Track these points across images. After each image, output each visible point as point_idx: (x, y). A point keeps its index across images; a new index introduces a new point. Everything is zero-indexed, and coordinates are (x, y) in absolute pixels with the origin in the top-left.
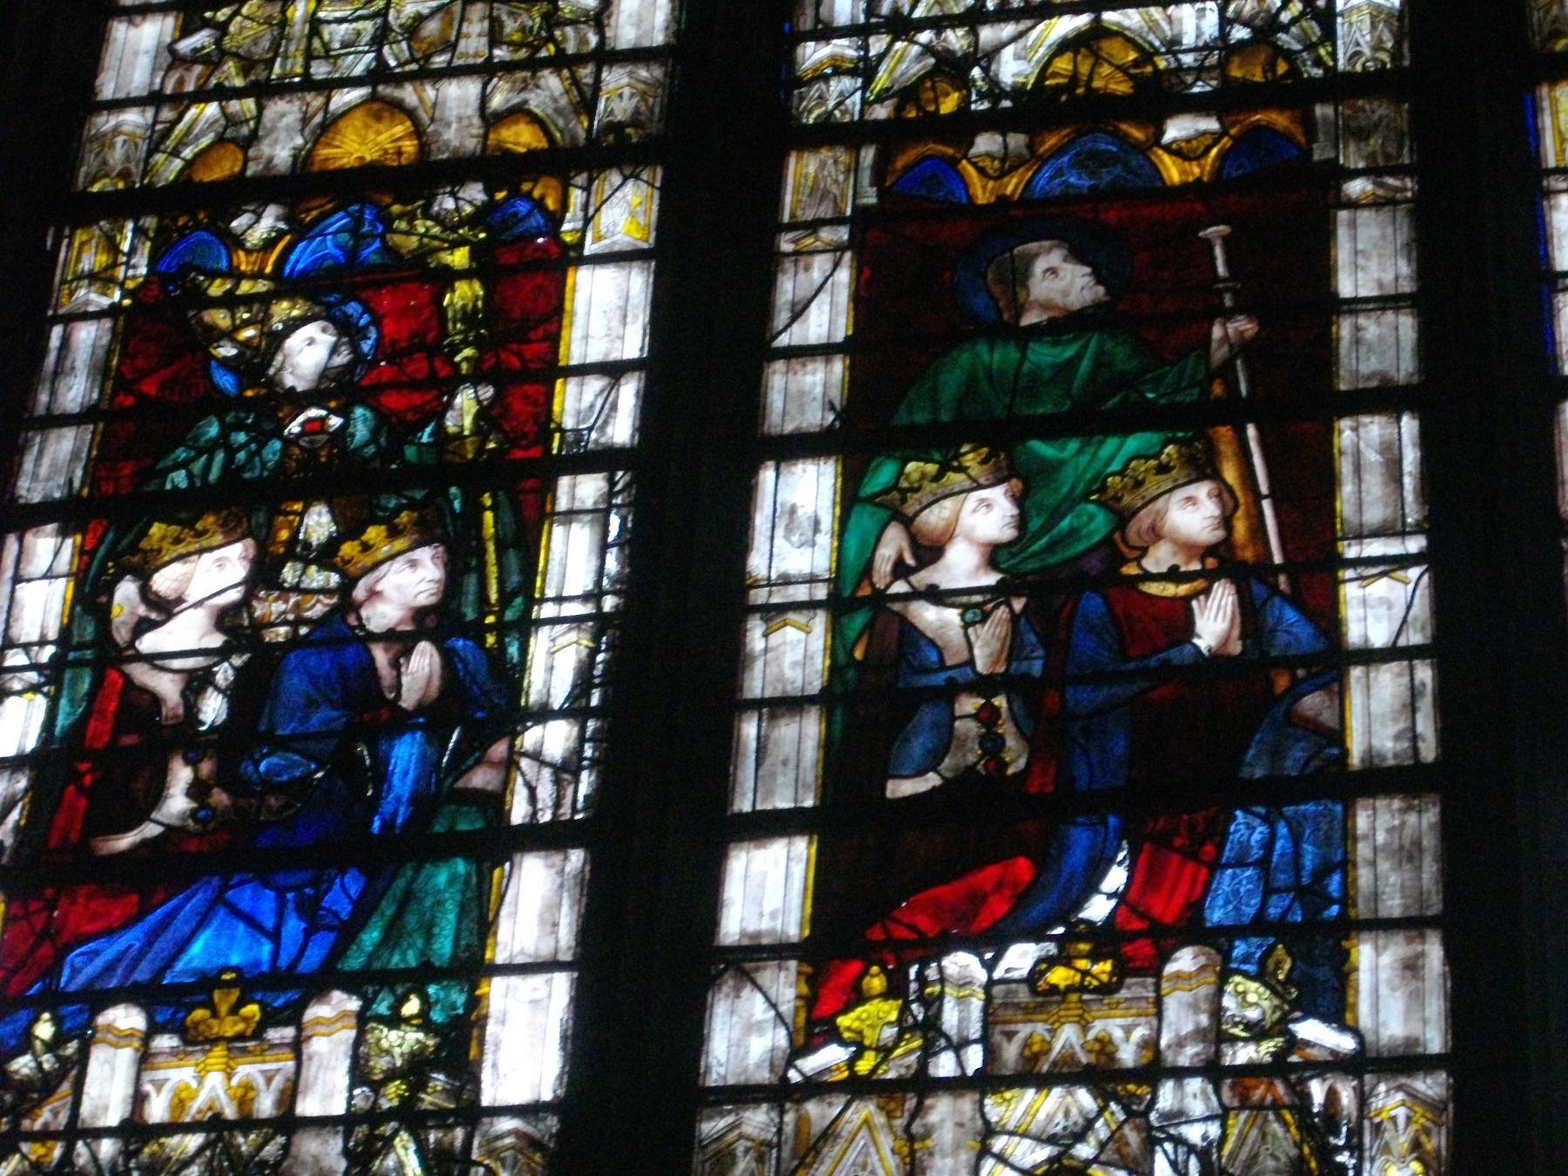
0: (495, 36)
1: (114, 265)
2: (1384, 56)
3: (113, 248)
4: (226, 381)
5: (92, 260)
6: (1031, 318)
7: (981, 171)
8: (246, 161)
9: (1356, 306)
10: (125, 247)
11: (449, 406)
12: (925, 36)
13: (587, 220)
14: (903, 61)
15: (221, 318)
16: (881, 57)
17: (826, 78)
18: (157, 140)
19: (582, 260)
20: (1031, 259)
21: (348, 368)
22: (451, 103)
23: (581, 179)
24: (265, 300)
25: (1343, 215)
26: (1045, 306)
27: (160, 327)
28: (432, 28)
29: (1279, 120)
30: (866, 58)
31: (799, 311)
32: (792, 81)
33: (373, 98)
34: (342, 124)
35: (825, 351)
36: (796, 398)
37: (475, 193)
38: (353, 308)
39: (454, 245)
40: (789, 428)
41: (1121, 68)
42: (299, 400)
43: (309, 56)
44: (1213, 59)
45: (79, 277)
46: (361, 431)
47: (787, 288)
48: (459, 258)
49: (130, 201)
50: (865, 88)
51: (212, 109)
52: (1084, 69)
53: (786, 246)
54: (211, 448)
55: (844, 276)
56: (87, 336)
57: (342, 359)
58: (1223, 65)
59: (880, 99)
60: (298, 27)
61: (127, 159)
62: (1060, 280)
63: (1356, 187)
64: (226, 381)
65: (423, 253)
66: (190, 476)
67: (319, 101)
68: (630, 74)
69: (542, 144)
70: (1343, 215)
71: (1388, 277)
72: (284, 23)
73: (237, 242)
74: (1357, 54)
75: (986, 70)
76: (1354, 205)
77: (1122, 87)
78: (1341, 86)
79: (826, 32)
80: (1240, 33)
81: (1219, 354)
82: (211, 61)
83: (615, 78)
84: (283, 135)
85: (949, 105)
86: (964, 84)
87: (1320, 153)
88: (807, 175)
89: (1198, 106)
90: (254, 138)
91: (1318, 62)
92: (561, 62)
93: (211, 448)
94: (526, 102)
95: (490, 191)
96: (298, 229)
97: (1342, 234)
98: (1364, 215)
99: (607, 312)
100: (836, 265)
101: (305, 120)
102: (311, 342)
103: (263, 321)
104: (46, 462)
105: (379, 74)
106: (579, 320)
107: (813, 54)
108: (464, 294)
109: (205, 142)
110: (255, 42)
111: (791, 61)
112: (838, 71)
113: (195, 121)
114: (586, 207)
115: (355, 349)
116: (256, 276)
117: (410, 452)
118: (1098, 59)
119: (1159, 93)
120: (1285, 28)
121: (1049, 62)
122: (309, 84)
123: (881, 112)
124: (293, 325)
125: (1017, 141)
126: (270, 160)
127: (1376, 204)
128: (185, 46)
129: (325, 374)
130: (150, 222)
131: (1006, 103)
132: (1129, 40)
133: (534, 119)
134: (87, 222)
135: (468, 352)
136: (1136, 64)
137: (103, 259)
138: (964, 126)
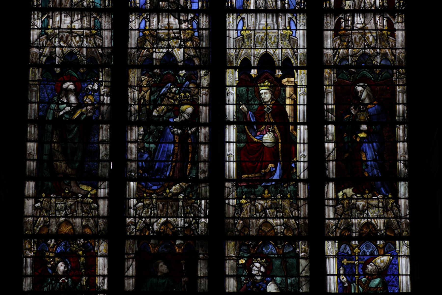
0: (83, 211)
1: (31, 248)
2: (205, 232)
3: (31, 244)
4: (50, 271)
5: (28, 246)
6: (159, 274)
7: (152, 246)
8: (48, 230)
9: (201, 277)
10: (33, 244)
11: (82, 280)
12: (144, 219)
13: (98, 248)
14: (141, 224)
15: (48, 259)
16: (138, 222)
17: (130, 226)
18: (34, 223)
19: (98, 256)
20: (159, 263)
21: (67, 271)
22: (77, 223)
23: (97, 240)
24: (54, 257)
25: (199, 261)
26: (161, 272)
27: (39, 260)
28: (73, 207)
29: (191, 242)
30: (135, 222)
31: (128, 269)
32: (125, 225)
33: (65, 221)
34: (62, 225)
35: (132, 277)
36: (129, 284)
37: (82, 240)
38: (67, 260)
39: (80, 251)
40: (128, 290)
41: (170, 229)
42: (61, 276)
43: (56, 210)
44: (183, 230)
45: (26, 249)
46: (70, 283)
47: (127, 265)
48: (81, 253)
49: (32, 236)
50: (136, 228)
51: (42, 219)
52: (165, 229)
53: (126, 257)
54: (49, 283)
55: (134, 263)
56: (29, 260)
57: (66, 269)
58: (184, 231)
59: (138, 231)
60: (53, 204)
61: (31, 227)
62: (163, 268)
63: (201, 256)
64: (50, 271)
65: (76, 252)
66: (47, 288)
67: (58, 220)
68: (103, 220)
69: (91, 233)
70: (199, 261)
71: (205, 272)
72: (51, 203)
73: (48, 245)
74: (202, 231)
75: (152, 227)
76: (201, 259)
77: (171, 233)
78: (200, 237)
79: (130, 217)
80: (186, 225)
81: (183, 283)
82: (41, 208)
83: (100, 221)
84: (53, 226)
85: (147, 233)
86: (149, 229)
87: (197, 249)
88: (128, 243)
89: (180, 238)
90: (49, 226)
91: (197, 232)
92: (93, 217)
93: (49, 283)
94: (88, 224)
95: (84, 241)
96: (57, 244)
97: (199, 264)
98: (202, 261)
99: (102, 265)
100: (133, 261)
101: (56, 223)
102: (61, 265)
103: (54, 261)
104: (26, 283)
105: (66, 216)
106: (98, 267)
107: (128, 220)
108: (82, 259)
109: (42, 225)
110: (47, 206)
111: (125, 221)
112: (132, 225)
113: (40, 221)
114: (98, 246)
115: (68, 268)
116: (52, 252)
117: (77, 287)
118: (167, 227)
119: (175, 235)
120: (192, 225)
121: (161, 227)
122: (56, 217)
123: (138, 234)
124: (59, 262)
125: (157, 241)
126: (52, 230)
127: (204, 259)
128: (37, 205)
129: (64, 272)
130: (36, 240)
131: (155, 234)
132: (172, 224)
133: (89, 228)
134: (26, 239)
135: (83, 270)
136: (173, 229)
137: (29, 246)
138: (149, 238)
